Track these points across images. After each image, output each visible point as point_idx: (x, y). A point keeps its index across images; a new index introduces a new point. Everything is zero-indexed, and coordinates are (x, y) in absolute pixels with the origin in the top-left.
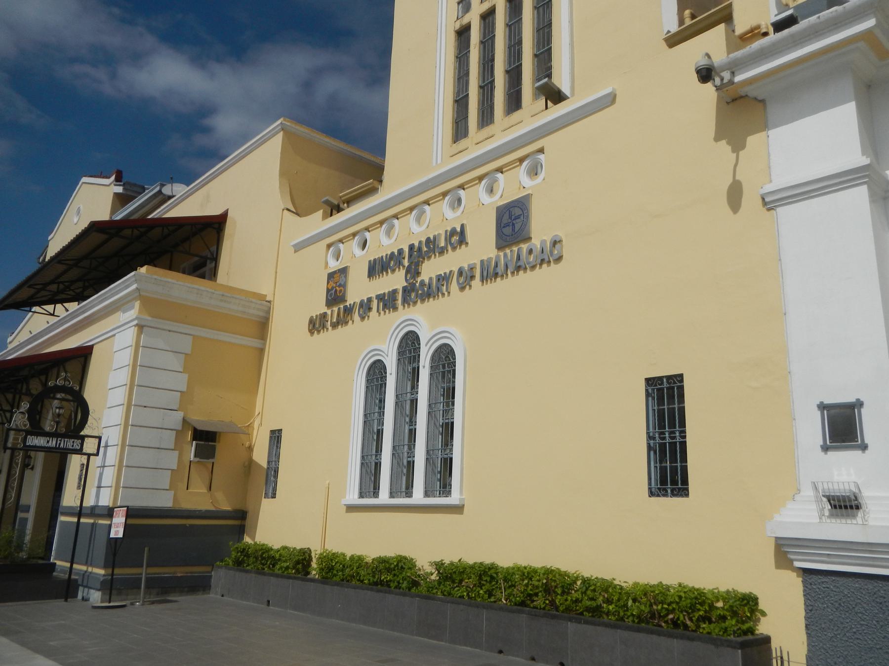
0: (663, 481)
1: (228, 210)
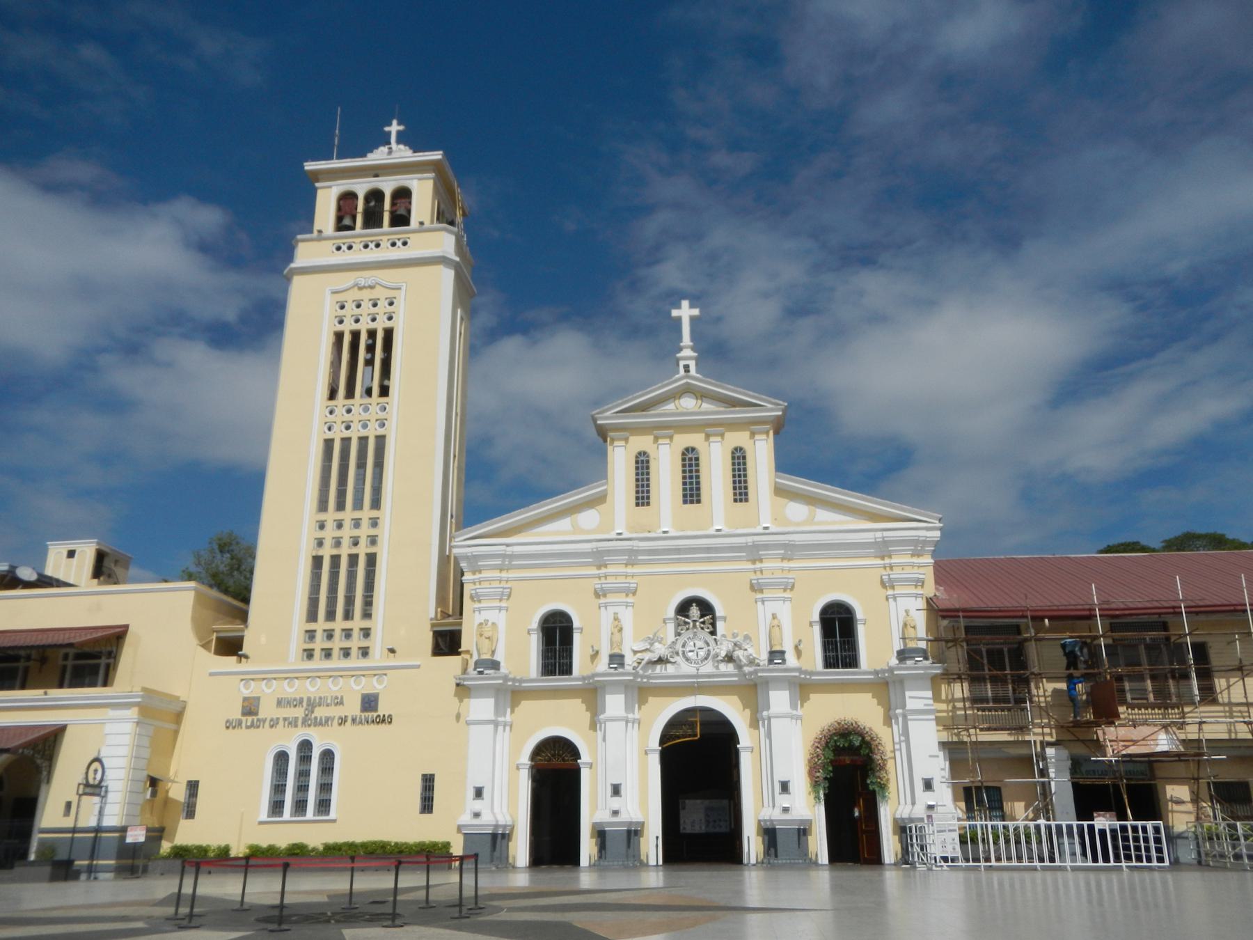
0: (425, 809)
1: (126, 627)
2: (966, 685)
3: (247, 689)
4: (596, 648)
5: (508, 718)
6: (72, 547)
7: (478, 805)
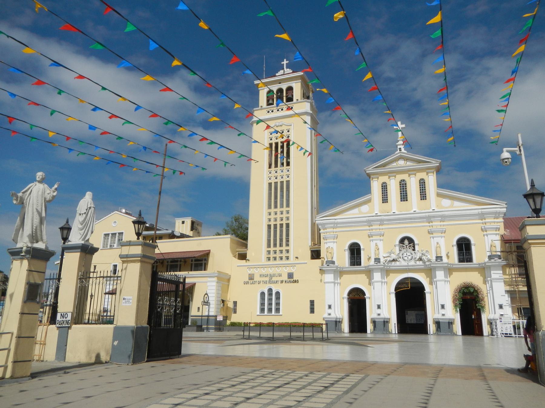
1: (210, 250)
2: (517, 268)
3: (250, 271)
4: (369, 256)
5: (339, 281)
6: (183, 220)
7: (330, 311)
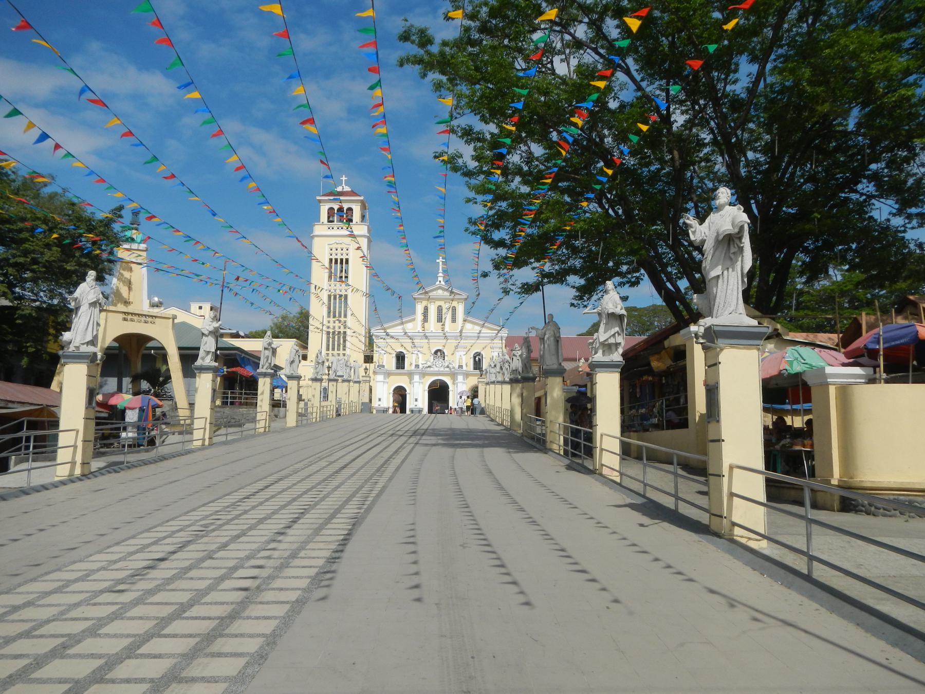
7: (379, 403)
